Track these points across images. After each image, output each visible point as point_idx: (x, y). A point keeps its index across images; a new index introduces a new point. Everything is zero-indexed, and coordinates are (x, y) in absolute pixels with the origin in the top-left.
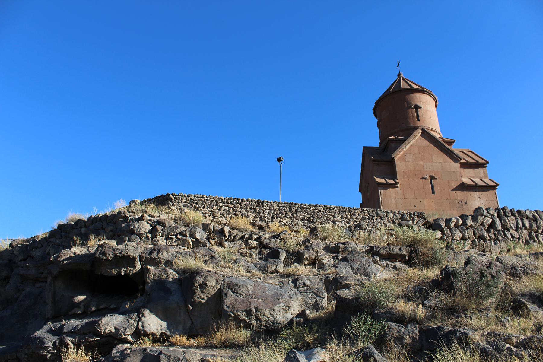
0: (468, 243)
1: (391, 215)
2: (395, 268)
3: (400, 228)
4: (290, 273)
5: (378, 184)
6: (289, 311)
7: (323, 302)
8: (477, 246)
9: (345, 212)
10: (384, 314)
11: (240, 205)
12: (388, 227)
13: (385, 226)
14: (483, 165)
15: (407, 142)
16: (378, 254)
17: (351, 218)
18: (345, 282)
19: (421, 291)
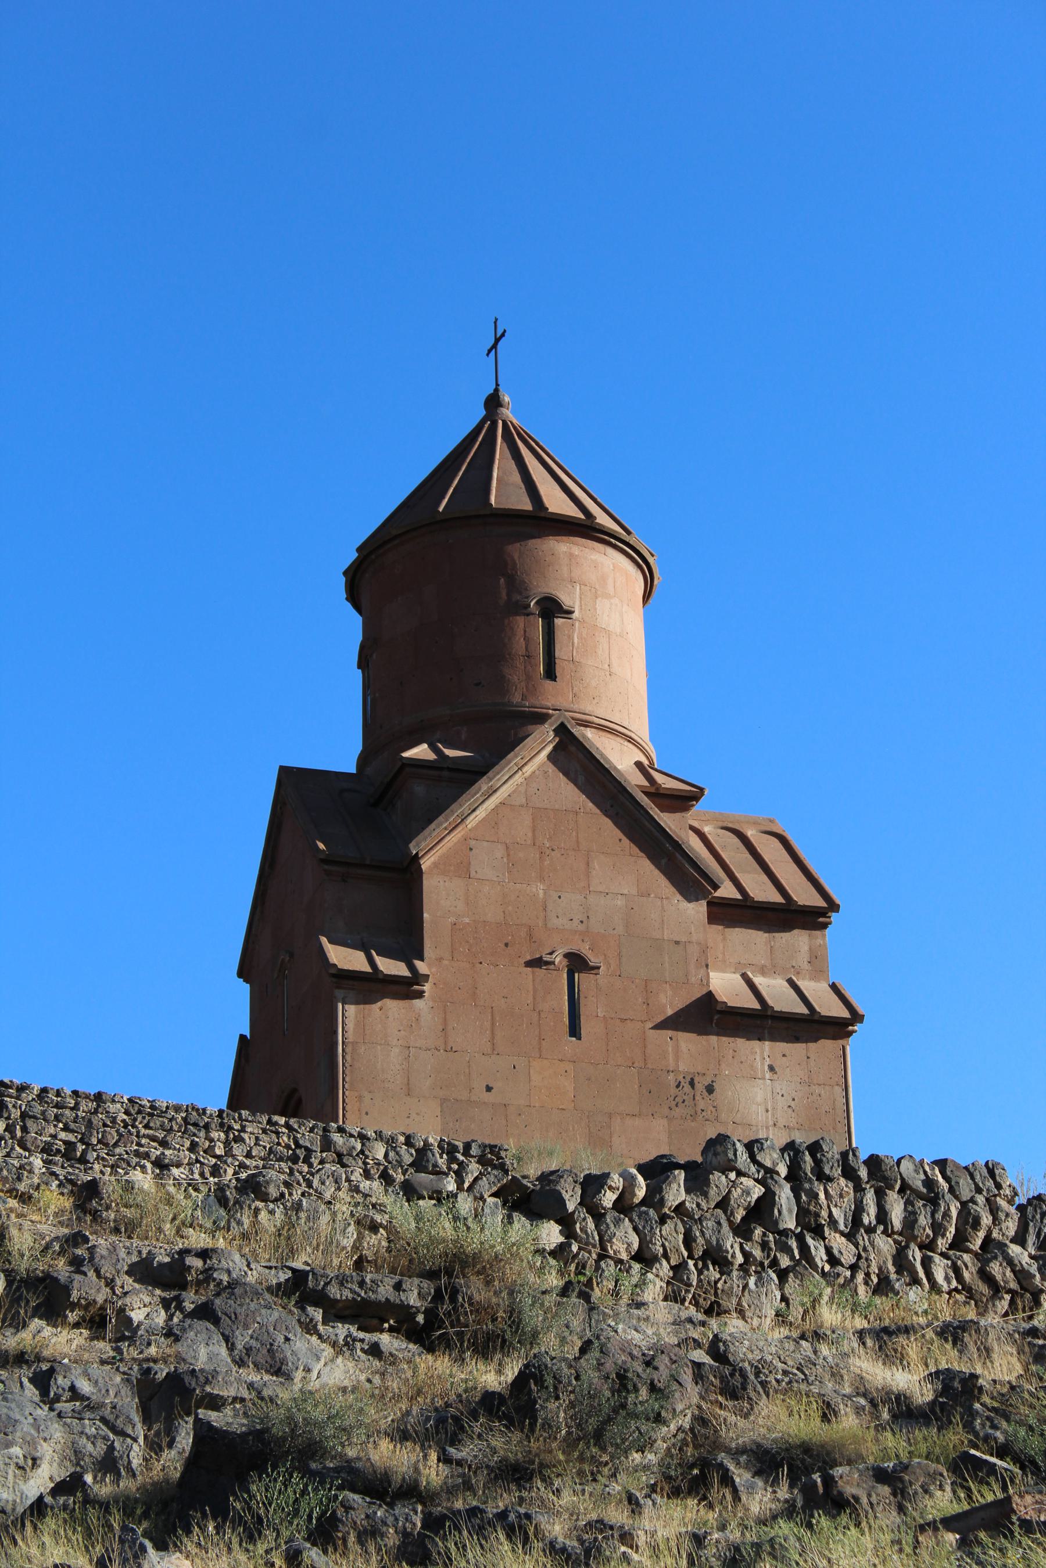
0: (657, 1276)
1: (379, 1151)
2: (375, 1351)
3: (408, 1201)
4: (22, 1354)
5: (333, 975)
6: (31, 1474)
7: (132, 1454)
8: (692, 1290)
9: (207, 1127)
10: (334, 1473)
12: (366, 1196)
13: (350, 1190)
15: (484, 788)
16: (320, 1299)
17: (229, 1152)
18: (208, 1389)
19: (441, 1421)
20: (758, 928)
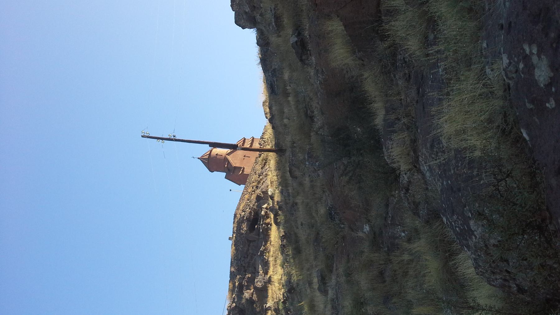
1: (255, 165)
14: (245, 139)
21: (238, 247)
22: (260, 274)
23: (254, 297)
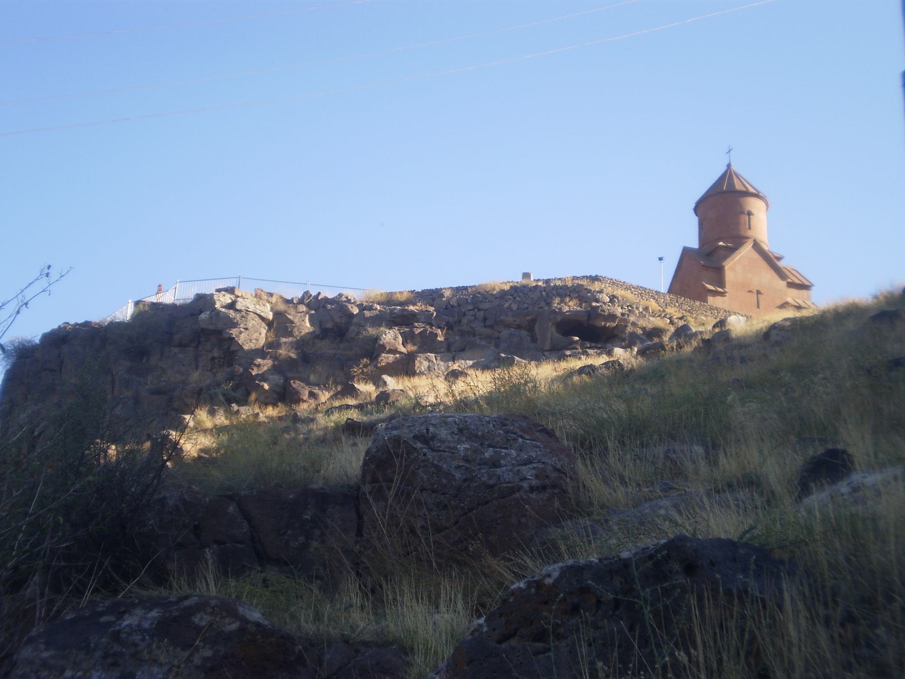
11: (645, 292)
20: (796, 289)
21: (510, 297)
22: (450, 363)
23: (388, 358)
